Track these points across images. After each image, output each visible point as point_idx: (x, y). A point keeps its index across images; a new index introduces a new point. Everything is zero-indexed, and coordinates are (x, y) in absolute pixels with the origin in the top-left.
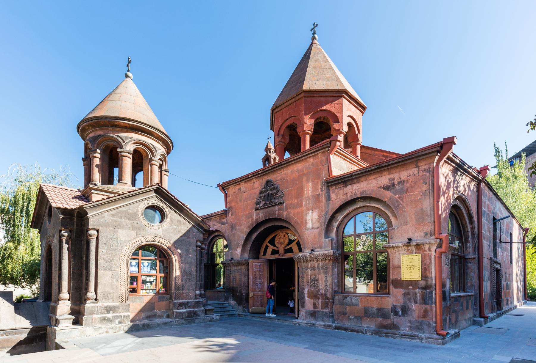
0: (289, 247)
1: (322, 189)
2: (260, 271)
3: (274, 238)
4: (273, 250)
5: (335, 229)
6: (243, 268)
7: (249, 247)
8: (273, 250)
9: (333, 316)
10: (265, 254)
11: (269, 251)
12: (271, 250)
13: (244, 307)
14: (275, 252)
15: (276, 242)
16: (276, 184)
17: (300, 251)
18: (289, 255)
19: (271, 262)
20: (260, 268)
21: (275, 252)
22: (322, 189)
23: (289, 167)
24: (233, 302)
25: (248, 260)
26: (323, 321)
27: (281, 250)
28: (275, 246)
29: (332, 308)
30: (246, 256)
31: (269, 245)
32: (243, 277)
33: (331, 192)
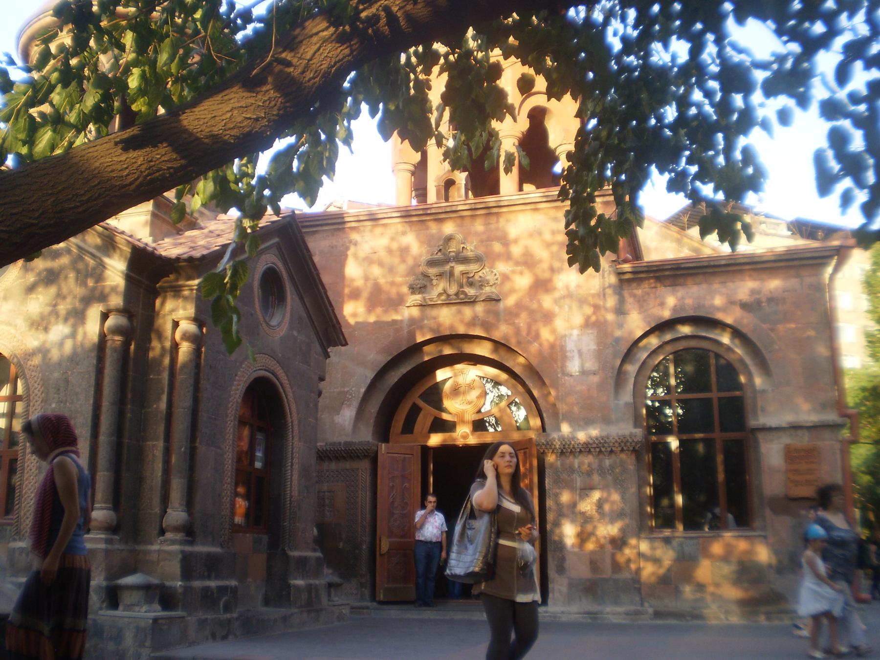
5: (632, 381)
7: (374, 407)
9: (639, 590)
11: (423, 421)
13: (362, 585)
26: (616, 602)
30: (366, 435)
31: (421, 404)
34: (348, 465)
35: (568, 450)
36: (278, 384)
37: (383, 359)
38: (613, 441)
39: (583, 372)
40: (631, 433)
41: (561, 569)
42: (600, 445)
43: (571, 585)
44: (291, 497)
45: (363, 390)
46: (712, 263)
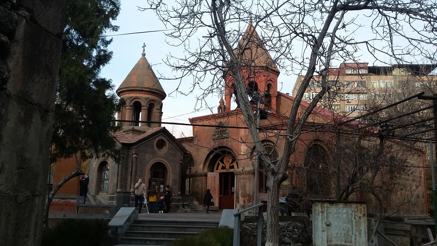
0: (232, 165)
3: (223, 159)
4: (223, 166)
6: (204, 178)
7: (207, 164)
8: (223, 166)
10: (217, 169)
11: (220, 167)
14: (223, 168)
15: (224, 161)
18: (232, 170)
19: (221, 174)
21: (223, 168)
27: (227, 167)
28: (224, 164)
29: (252, 202)
30: (206, 170)
31: (220, 162)
32: (204, 185)
34: (201, 178)
37: (208, 153)
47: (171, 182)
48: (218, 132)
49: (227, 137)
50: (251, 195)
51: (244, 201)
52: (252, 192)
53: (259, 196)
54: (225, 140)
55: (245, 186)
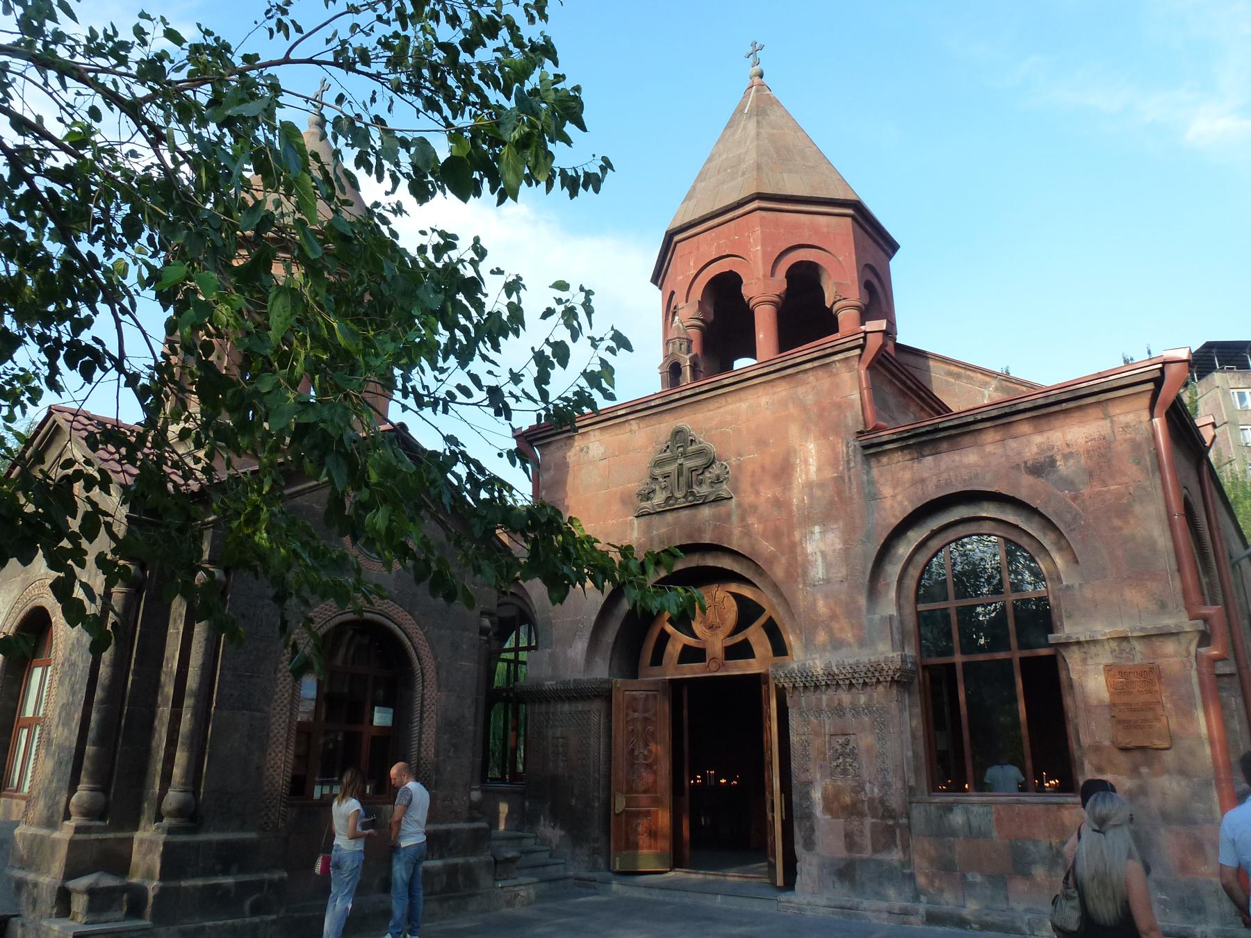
0: (739, 638)
1: (848, 462)
2: (646, 719)
4: (686, 648)
6: (596, 706)
7: (610, 636)
8: (686, 648)
10: (657, 659)
12: (679, 647)
13: (595, 851)
16: (703, 441)
17: (780, 648)
19: (676, 685)
20: (646, 711)
22: (848, 462)
23: (742, 395)
24: (553, 833)
25: (608, 681)
28: (694, 635)
30: (601, 671)
31: (669, 628)
33: (875, 472)
34: (580, 706)
35: (813, 685)
36: (393, 626)
38: (864, 670)
39: (827, 581)
40: (886, 658)
41: (809, 845)
42: (849, 676)
43: (822, 866)
44: (419, 759)
45: (594, 618)
46: (979, 417)
47: (429, 735)
48: (666, 476)
49: (719, 500)
50: (895, 802)
51: (848, 836)
52: (898, 784)
53: (949, 808)
54: (706, 512)
55: (846, 753)
